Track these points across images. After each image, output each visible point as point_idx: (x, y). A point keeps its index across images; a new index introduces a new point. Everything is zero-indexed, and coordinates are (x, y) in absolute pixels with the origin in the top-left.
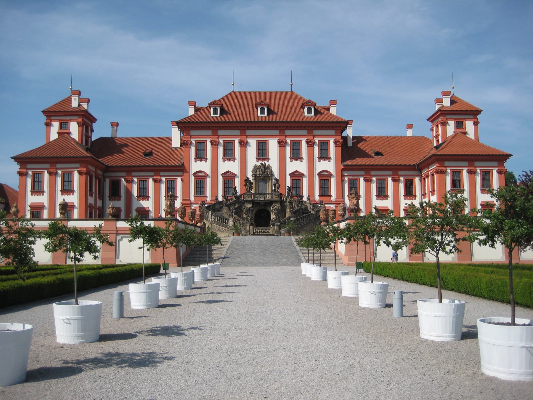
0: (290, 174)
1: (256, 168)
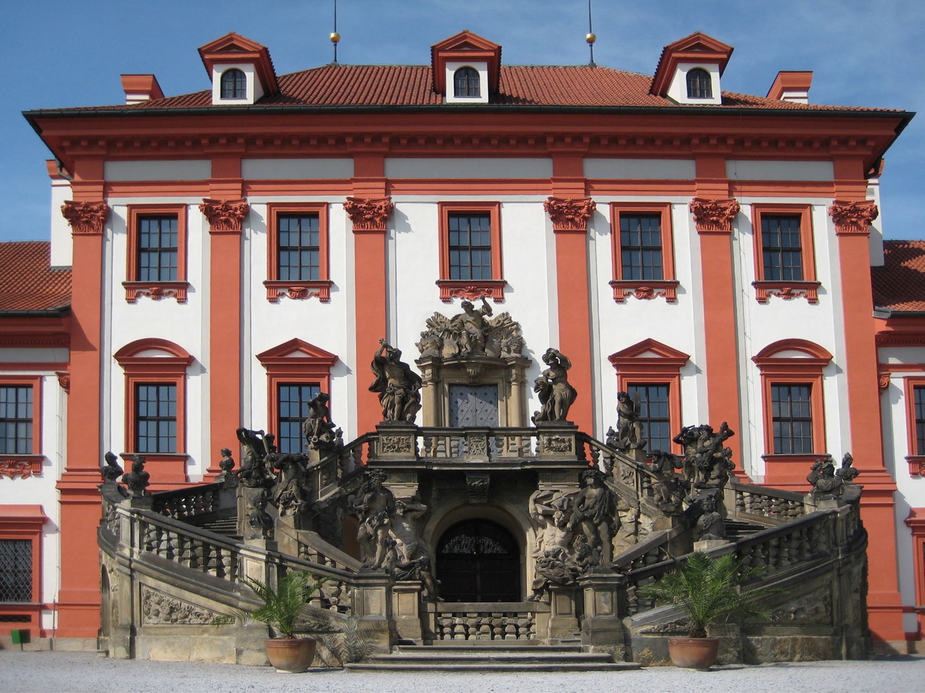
0: (613, 358)
1: (437, 332)
